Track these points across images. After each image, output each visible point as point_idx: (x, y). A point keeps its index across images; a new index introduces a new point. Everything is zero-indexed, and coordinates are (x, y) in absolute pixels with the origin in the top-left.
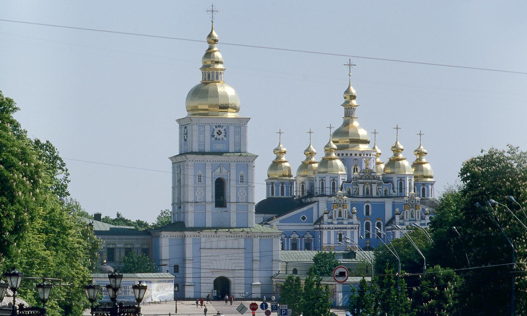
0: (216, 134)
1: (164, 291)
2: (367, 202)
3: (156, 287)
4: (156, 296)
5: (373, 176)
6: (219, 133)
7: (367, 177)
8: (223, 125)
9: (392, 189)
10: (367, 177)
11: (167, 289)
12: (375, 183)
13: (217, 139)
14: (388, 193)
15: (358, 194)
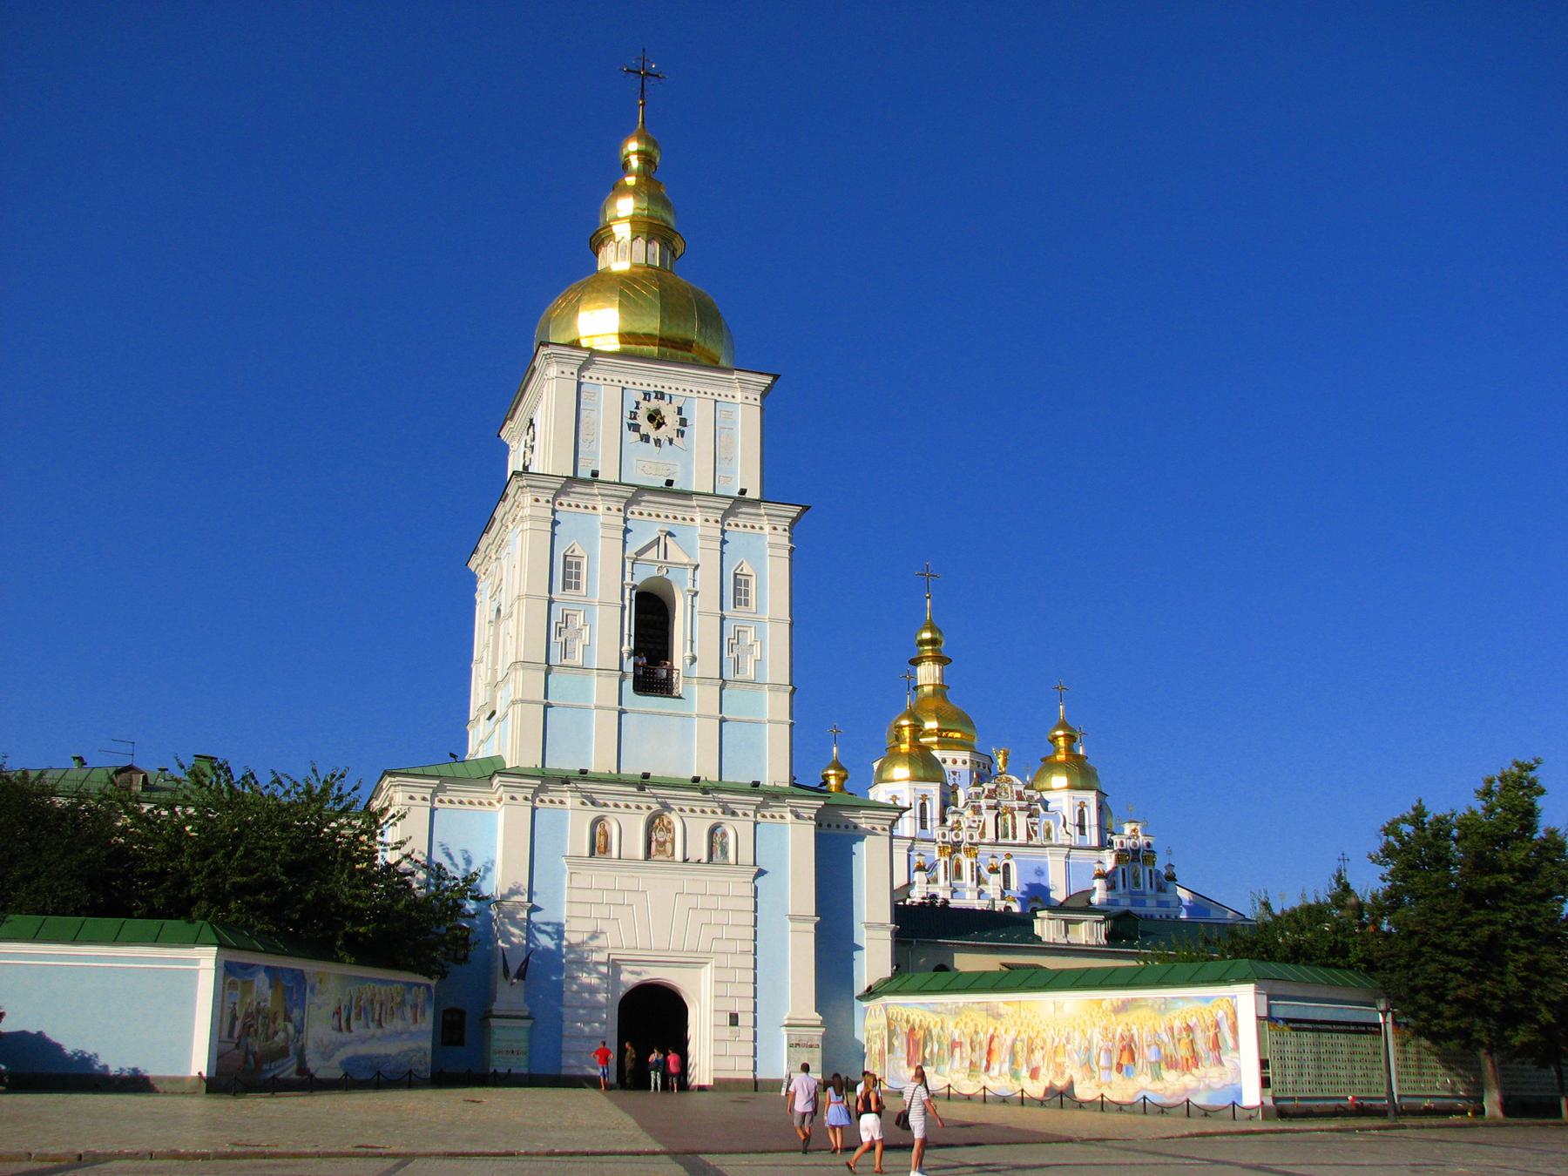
0: (642, 420)
1: (379, 1032)
2: (1009, 856)
3: (332, 1008)
4: (327, 1054)
5: (1017, 792)
6: (655, 418)
7: (1003, 794)
8: (673, 392)
9: (1064, 825)
10: (1003, 794)
11: (398, 1024)
12: (1021, 809)
13: (647, 441)
14: (1053, 835)
15: (983, 835)
